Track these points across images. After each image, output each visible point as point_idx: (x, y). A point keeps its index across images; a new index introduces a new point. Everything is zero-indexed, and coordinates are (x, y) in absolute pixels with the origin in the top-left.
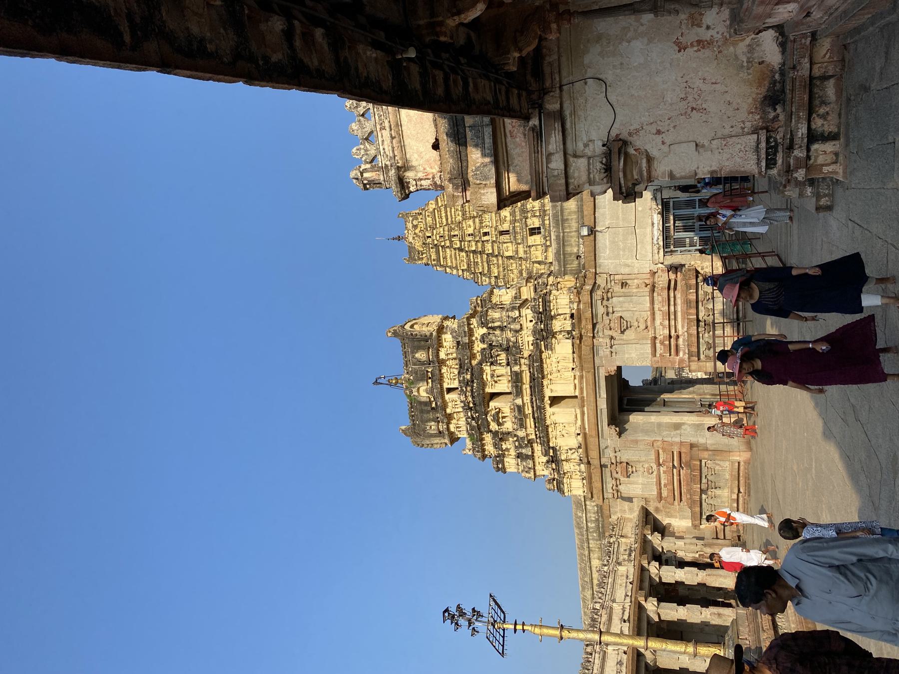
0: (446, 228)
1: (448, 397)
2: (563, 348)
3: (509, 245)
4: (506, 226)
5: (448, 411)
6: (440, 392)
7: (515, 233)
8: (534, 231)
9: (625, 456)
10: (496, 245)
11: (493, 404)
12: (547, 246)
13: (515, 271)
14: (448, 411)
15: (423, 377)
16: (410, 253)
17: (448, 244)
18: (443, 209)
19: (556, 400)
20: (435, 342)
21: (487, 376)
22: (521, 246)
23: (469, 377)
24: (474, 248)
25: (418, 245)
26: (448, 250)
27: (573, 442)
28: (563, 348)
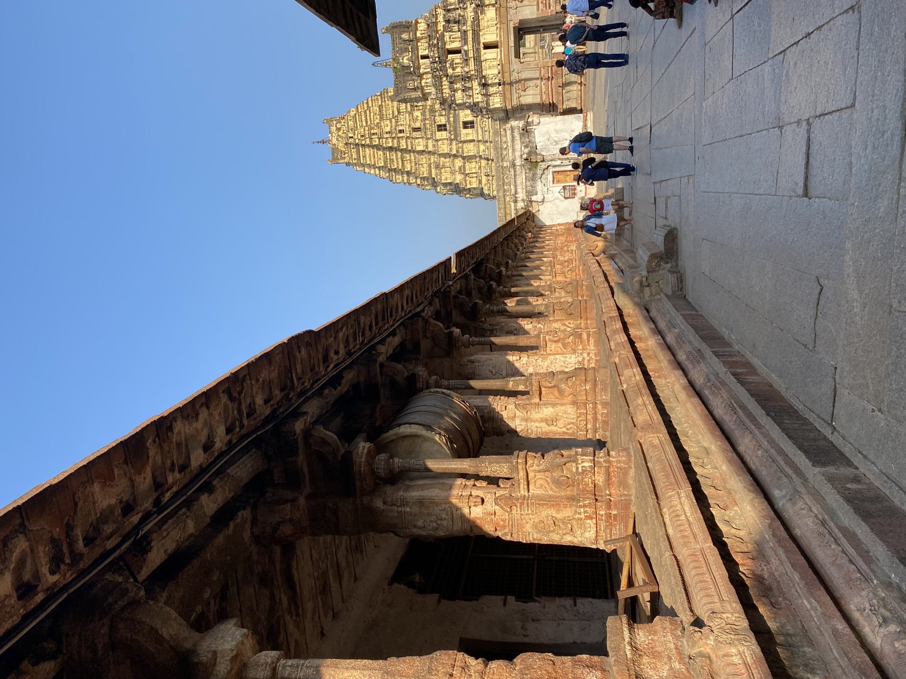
1: (421, 61)
2: (491, 13)
3: (420, 140)
4: (418, 125)
5: (422, 71)
6: (416, 58)
7: (426, 129)
8: (442, 127)
9: (524, 75)
10: (409, 141)
11: (450, 56)
12: (451, 140)
13: (425, 165)
15: (406, 50)
16: (333, 154)
19: (487, 47)
20: (414, 29)
21: (447, 38)
22: (430, 141)
23: (435, 42)
24: (390, 145)
25: (341, 146)
26: (367, 149)
27: (496, 71)
28: (491, 13)
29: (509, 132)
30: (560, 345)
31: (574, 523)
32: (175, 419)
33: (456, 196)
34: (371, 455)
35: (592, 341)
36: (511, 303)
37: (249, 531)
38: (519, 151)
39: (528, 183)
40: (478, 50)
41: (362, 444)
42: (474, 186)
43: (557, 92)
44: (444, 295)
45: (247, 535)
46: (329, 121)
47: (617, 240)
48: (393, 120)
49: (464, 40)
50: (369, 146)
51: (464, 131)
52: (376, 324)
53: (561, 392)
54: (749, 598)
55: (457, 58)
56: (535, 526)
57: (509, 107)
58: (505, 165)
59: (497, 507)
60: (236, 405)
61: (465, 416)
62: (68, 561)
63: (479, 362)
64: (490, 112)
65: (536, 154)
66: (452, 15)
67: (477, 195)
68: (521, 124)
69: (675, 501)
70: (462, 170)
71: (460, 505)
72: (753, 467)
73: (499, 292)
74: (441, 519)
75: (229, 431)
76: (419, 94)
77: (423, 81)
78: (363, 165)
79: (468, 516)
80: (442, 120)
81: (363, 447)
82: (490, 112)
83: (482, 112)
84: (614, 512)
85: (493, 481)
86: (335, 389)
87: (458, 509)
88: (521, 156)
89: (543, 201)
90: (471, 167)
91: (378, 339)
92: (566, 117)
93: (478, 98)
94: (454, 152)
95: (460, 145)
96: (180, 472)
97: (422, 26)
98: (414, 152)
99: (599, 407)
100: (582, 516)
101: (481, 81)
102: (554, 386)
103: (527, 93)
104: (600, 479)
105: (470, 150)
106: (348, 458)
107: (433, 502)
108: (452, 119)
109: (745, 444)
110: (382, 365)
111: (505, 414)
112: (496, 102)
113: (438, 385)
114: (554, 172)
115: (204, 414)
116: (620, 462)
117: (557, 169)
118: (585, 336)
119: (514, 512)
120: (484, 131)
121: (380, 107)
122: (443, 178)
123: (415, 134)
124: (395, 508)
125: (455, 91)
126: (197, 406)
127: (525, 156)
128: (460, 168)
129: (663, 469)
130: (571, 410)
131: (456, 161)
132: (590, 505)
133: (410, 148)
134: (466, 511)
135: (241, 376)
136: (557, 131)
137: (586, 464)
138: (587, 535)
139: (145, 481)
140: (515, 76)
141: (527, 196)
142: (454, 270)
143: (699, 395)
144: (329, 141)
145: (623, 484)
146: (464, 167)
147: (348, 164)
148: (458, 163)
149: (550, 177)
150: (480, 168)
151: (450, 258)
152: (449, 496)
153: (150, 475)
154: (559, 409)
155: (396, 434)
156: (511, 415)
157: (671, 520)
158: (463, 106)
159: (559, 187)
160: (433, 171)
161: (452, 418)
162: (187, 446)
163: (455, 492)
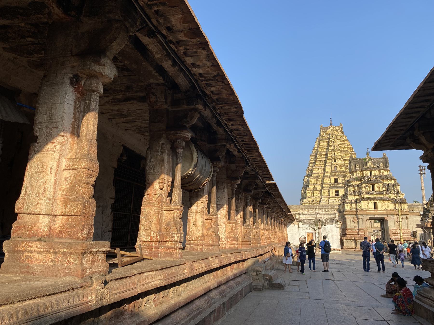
0: (337, 144)
1: (369, 172)
2: (391, 206)
3: (330, 170)
4: (338, 169)
5: (364, 172)
6: (371, 169)
9: (360, 221)
11: (371, 186)
12: (330, 185)
13: (318, 171)
14: (364, 172)
15: (374, 165)
16: (325, 127)
17: (330, 144)
18: (344, 143)
19: (375, 204)
21: (380, 184)
22: (330, 174)
23: (378, 179)
24: (329, 155)
25: (329, 131)
26: (327, 144)
27: (363, 207)
29: (333, 212)
30: (230, 230)
31: (149, 231)
32: (207, 51)
33: (303, 186)
34: (185, 139)
35: (232, 246)
36: (250, 208)
37: (153, 82)
38: (323, 216)
39: (308, 221)
40: (374, 199)
41: (190, 135)
42: (307, 195)
43: (351, 237)
44: (256, 176)
45: (151, 81)
46: (341, 126)
47: (279, 262)
48: (340, 157)
49: (378, 193)
50: (328, 145)
51: (334, 191)
52: (244, 144)
53: (209, 229)
54: (115, 308)
55: (370, 189)
56: (149, 213)
57: (345, 213)
58: (317, 210)
59: (158, 196)
60: (212, 78)
61: (200, 183)
62: (149, 3)
63: (224, 191)
64: (343, 204)
65: (322, 225)
66: (391, 188)
67: (303, 196)
68: (337, 219)
69: (159, 277)
70: (315, 189)
71: (160, 178)
72: (171, 316)
73: (256, 203)
74: (154, 170)
75: (200, 75)
76: (353, 170)
77: (359, 172)
78: (319, 142)
79: (155, 182)
80: (340, 181)
81: (189, 135)
82: (343, 204)
83: (343, 200)
84: (153, 250)
85: (170, 194)
86: (215, 124)
87: (158, 177)
88: (321, 218)
89: (299, 227)
90: (317, 194)
91: (237, 145)
92: (339, 240)
93: (350, 198)
94: (324, 186)
95: (327, 189)
96: (183, 52)
97: (386, 173)
98: (325, 166)
99: (201, 247)
100: (152, 235)
101: (358, 200)
102: (211, 226)
103: (352, 222)
104: (169, 244)
105: (325, 193)
106: (183, 128)
107: (162, 166)
108: (340, 185)
109: (182, 313)
110: (225, 146)
111: (199, 202)
112: (348, 207)
113: (214, 171)
114: (313, 233)
115: (209, 64)
116: (177, 254)
117: (314, 235)
118: (234, 242)
119: (156, 203)
120: (334, 200)
121: (347, 151)
122: (312, 180)
123: (333, 167)
124: (160, 149)
125: (354, 187)
126: (213, 61)
127: (321, 219)
128: (316, 188)
129: (173, 273)
130: (200, 233)
131: (320, 186)
132: (157, 239)
133: (327, 164)
134: (157, 181)
135: (225, 81)
136: (333, 236)
137: (176, 238)
138: (143, 237)
139: (181, 37)
140: (360, 217)
141: (301, 220)
142: (267, 182)
143: (205, 294)
144: (331, 126)
145: (166, 255)
146: (317, 190)
147: (320, 134)
148: (319, 187)
149: (310, 231)
150: (316, 198)
151: (274, 180)
152: (165, 174)
153: (184, 39)
154: (201, 228)
155: (193, 150)
156: (199, 205)
157: (150, 275)
158: (346, 191)
159: (305, 235)
160: (315, 175)
161: (199, 177)
162: (195, 56)
163: (166, 176)
